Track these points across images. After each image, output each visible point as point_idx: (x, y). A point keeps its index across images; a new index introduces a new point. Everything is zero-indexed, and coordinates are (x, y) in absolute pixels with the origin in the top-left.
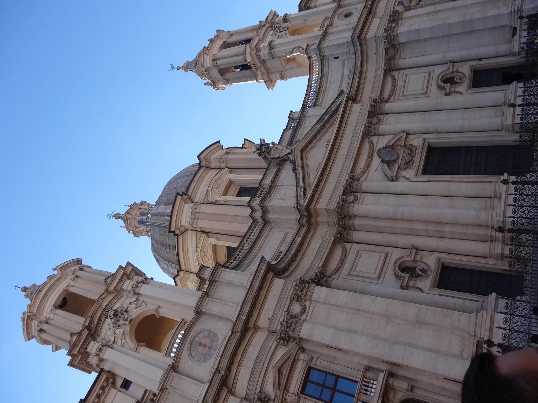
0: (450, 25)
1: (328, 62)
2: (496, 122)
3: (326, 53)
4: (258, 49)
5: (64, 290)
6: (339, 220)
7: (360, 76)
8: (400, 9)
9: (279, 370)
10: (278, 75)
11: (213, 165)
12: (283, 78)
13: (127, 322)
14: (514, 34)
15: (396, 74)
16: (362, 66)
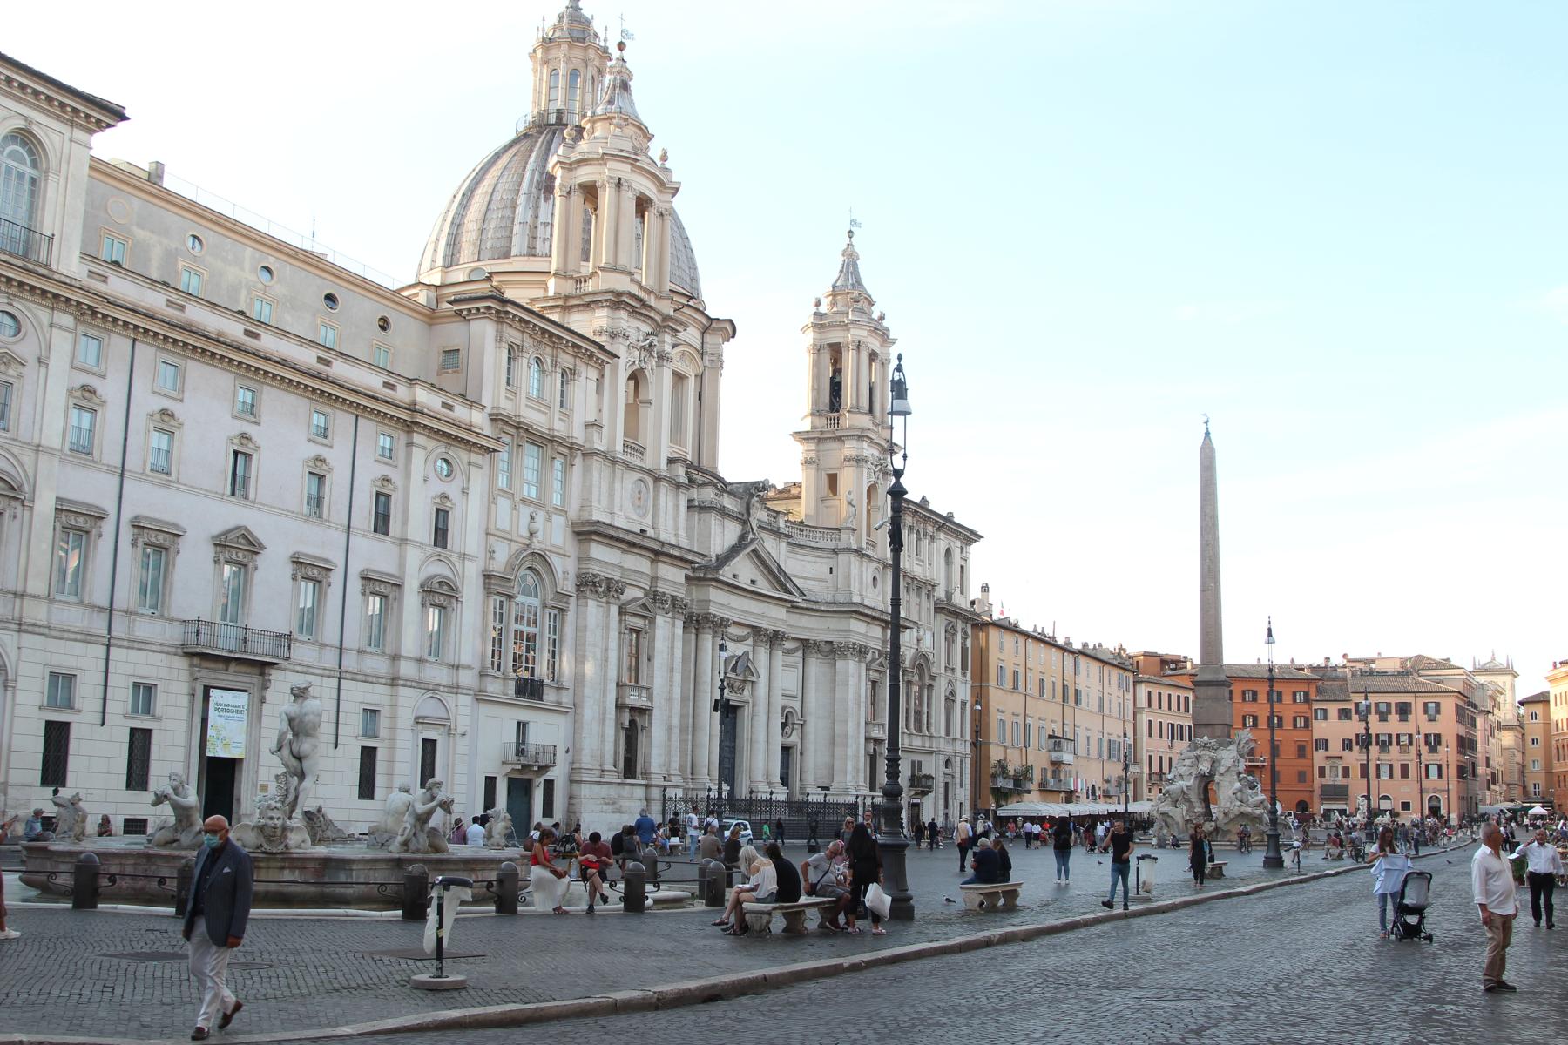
0: (846, 722)
1: (828, 557)
2: (759, 775)
3: (842, 558)
4: (860, 437)
5: (651, 200)
6: (699, 616)
7: (807, 609)
8: (869, 657)
9: (644, 606)
10: (813, 455)
11: (708, 338)
12: (807, 462)
13: (643, 365)
14: (824, 788)
15: (800, 653)
16: (817, 611)
